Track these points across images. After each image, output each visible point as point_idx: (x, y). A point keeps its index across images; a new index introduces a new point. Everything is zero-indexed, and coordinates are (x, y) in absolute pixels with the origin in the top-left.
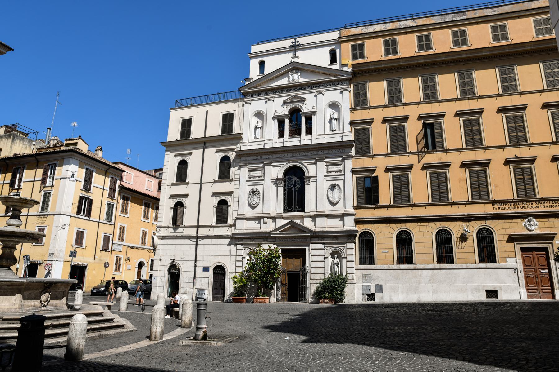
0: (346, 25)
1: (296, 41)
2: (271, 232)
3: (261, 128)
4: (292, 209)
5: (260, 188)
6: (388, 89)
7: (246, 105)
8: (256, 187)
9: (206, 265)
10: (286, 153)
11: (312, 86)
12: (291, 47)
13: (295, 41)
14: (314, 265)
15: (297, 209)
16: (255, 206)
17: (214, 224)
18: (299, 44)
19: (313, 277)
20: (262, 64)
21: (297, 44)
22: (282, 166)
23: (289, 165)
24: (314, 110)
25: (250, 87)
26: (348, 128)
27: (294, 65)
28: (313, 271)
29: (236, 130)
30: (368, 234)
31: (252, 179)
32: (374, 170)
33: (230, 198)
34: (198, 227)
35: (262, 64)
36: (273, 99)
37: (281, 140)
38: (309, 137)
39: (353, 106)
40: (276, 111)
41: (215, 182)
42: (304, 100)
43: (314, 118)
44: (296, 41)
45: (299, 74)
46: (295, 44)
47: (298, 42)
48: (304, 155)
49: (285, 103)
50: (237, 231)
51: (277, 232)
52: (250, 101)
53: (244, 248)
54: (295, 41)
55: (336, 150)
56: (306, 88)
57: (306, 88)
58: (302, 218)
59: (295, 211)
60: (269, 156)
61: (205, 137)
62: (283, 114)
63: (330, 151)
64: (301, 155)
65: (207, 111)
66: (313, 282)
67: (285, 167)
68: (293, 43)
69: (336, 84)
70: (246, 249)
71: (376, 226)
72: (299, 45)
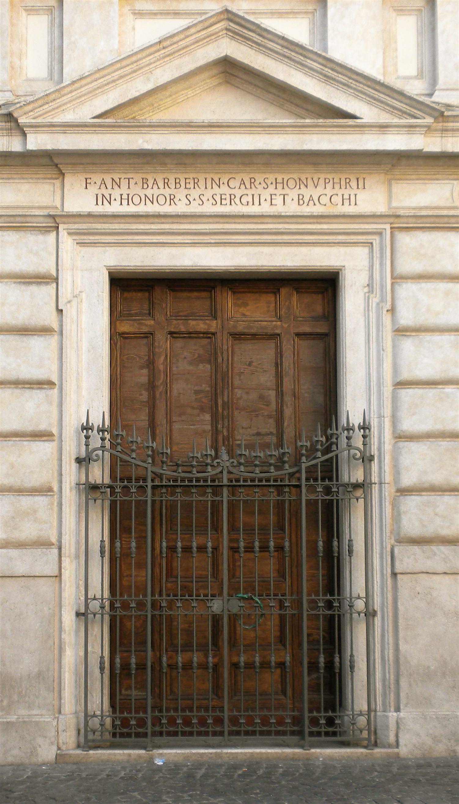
66: (429, 565)
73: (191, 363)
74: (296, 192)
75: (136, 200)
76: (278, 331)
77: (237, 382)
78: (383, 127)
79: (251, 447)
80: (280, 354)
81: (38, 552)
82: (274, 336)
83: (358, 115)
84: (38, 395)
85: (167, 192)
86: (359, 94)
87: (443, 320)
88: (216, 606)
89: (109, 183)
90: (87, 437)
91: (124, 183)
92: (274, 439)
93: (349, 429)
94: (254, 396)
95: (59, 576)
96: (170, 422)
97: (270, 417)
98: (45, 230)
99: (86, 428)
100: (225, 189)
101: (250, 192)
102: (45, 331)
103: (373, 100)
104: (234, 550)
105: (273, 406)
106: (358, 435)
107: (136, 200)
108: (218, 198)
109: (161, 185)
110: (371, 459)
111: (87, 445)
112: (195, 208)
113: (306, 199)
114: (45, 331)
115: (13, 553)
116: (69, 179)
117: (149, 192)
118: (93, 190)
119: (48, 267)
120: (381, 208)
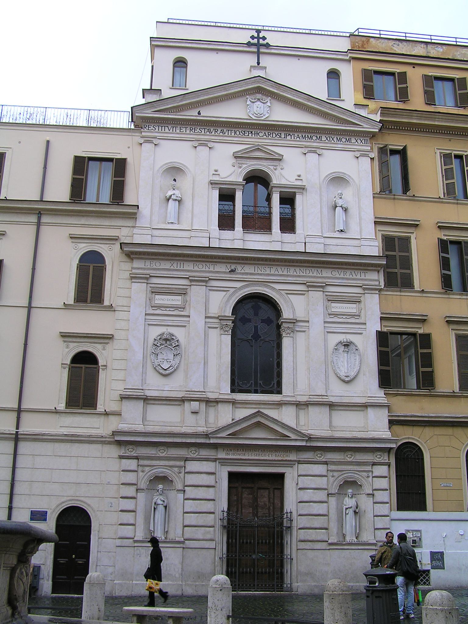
0: (360, 30)
1: (261, 35)
2: (211, 433)
3: (179, 201)
4: (251, 386)
5: (179, 333)
6: (444, 168)
7: (147, 147)
8: (172, 330)
9: (40, 505)
10: (239, 263)
11: (296, 135)
12: (249, 44)
13: (258, 35)
14: (305, 509)
15: (239, 385)
16: (167, 372)
17: (62, 406)
18: (267, 43)
19: (303, 535)
20: (180, 63)
21: (261, 41)
22: (232, 290)
23: (249, 289)
24: (299, 183)
25: (156, 110)
26: (369, 230)
27: (259, 82)
28: (303, 522)
29: (130, 198)
30: (407, 447)
31: (158, 312)
32: (423, 321)
33: (104, 349)
34: (19, 411)
35: (180, 63)
36: (210, 145)
37: (227, 234)
38: (288, 237)
39: (378, 190)
40: (216, 171)
41: (66, 306)
42: (279, 159)
43: (299, 199)
44: (261, 35)
45: (269, 104)
46: (258, 41)
47: (264, 38)
48: (281, 273)
49: (237, 156)
50: (124, 427)
51: (224, 434)
52: (155, 138)
53: (140, 469)
54: (258, 35)
55: (348, 272)
56: (283, 136)
57: (283, 136)
58: (279, 405)
59: (256, 392)
60: (201, 266)
61: (41, 201)
62: (231, 179)
63: (336, 273)
64: (272, 272)
65: (48, 142)
67: (237, 295)
68: (253, 37)
69: (344, 140)
70: (147, 469)
71: (428, 431)
72: (267, 46)
73: (247, 495)
74: (275, 453)
75: (236, 454)
76: (269, 487)
77: (259, 500)
78: (296, 440)
79: (263, 517)
80: (269, 493)
81: (211, 542)
82: (268, 489)
83: (290, 436)
84: (211, 502)
85: (243, 453)
86: (290, 431)
87: (310, 486)
88: (254, 556)
89: (229, 450)
90: (223, 514)
91: (233, 450)
92: (267, 515)
93: (287, 513)
94: (263, 504)
95: (215, 549)
96: (242, 510)
97: (267, 509)
98: (214, 461)
99: (223, 511)
100: (257, 452)
101: (263, 453)
102: (213, 487)
103: (293, 433)
104: (258, 543)
105: (268, 506)
106: (289, 514)
107: (236, 454)
108: (256, 455)
109: (242, 451)
110: (292, 520)
111: (223, 516)
112: (250, 457)
113: (277, 455)
114: (213, 487)
115: (205, 542)
116: (219, 449)
117: (239, 453)
118: (225, 452)
119: (213, 470)
120: (295, 459)
